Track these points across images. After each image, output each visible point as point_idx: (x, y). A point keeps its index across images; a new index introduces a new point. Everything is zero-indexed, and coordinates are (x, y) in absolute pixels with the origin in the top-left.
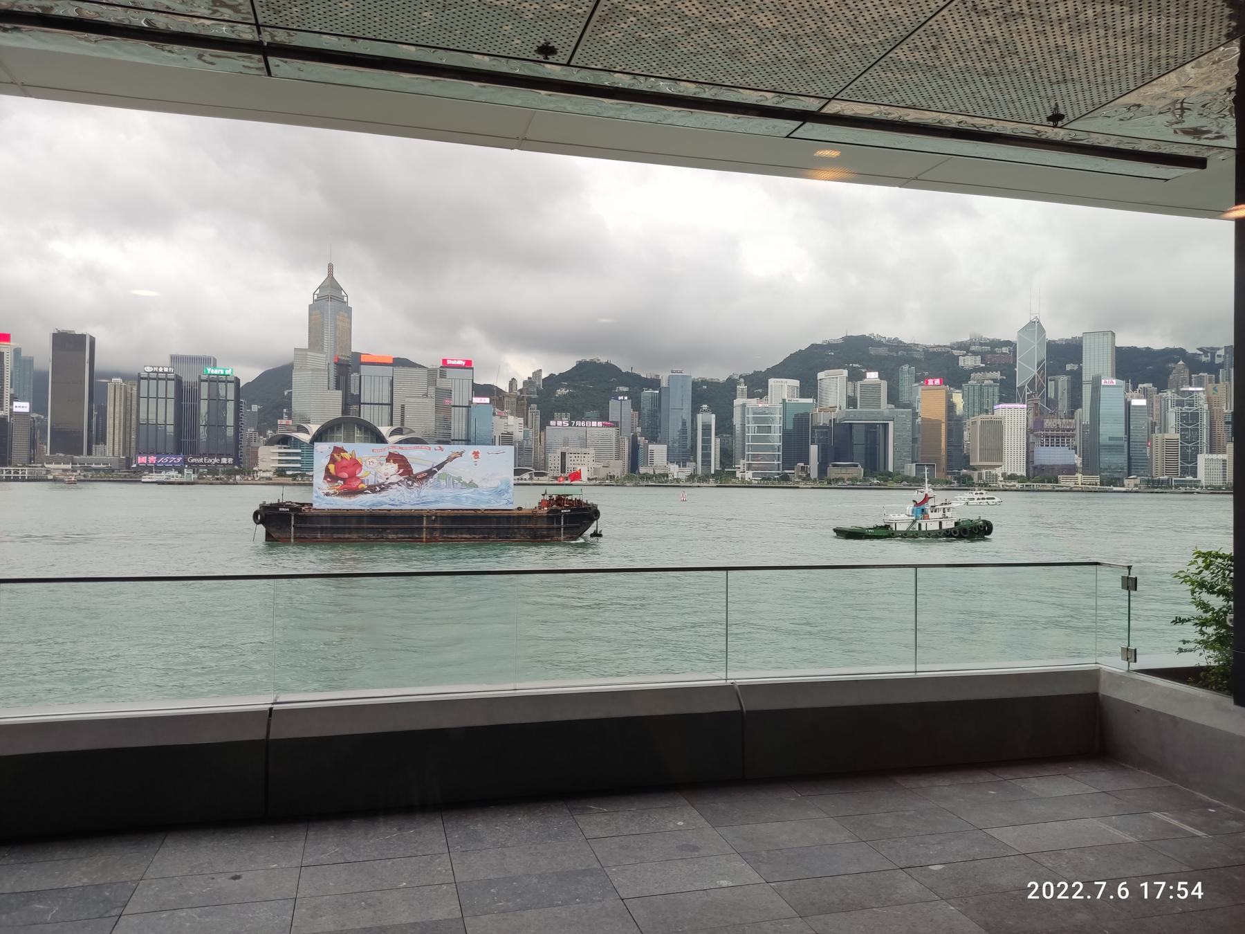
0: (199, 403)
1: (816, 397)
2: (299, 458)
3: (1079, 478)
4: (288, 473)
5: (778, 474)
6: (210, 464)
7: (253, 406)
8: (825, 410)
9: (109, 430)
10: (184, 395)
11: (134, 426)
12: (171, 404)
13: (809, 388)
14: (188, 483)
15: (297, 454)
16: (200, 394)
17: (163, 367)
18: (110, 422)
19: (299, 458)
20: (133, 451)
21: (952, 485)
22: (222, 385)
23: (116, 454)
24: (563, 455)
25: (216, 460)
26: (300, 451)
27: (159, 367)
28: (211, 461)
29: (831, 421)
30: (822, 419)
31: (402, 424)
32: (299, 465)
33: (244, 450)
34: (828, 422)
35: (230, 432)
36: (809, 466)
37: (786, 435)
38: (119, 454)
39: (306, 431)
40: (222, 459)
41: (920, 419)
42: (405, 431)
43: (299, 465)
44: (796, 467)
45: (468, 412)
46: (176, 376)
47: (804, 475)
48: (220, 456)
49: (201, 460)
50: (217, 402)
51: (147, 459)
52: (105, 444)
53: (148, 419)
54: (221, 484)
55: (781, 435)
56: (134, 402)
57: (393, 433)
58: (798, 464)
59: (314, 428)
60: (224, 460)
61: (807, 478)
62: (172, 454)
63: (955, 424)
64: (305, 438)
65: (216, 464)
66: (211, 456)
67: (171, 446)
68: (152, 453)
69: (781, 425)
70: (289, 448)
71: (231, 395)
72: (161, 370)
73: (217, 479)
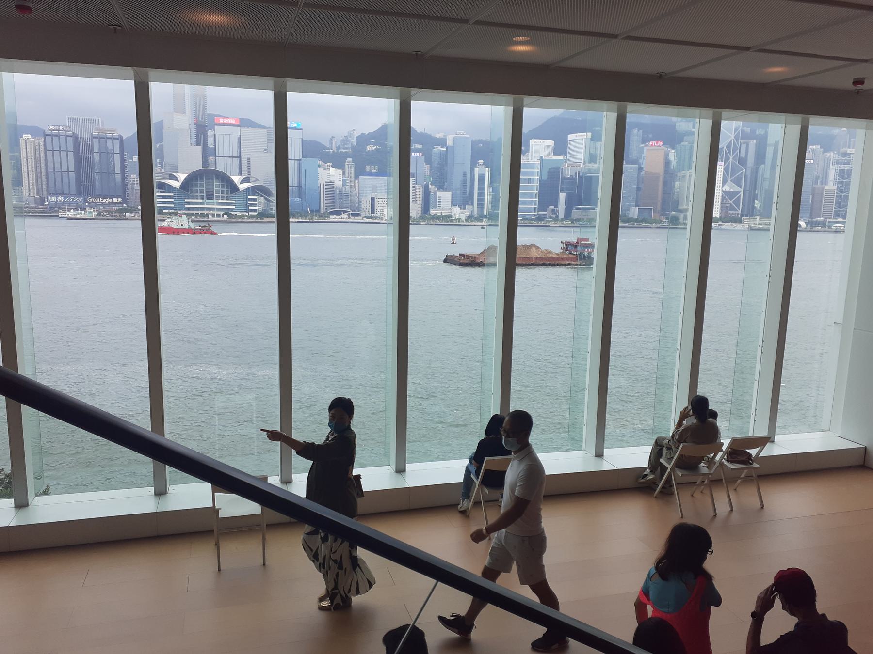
0: (93, 155)
1: (565, 154)
2: (172, 200)
3: (758, 220)
4: (164, 211)
5: (535, 215)
6: (105, 203)
7: (133, 157)
8: (572, 165)
9: (25, 175)
10: (80, 148)
11: (43, 172)
12: (71, 156)
13: (561, 148)
14: (90, 219)
15: (170, 197)
16: (93, 148)
17: (62, 127)
18: (24, 170)
19: (172, 200)
20: (45, 192)
21: (664, 224)
22: (109, 142)
23: (32, 194)
24: (373, 199)
25: (109, 200)
26: (172, 194)
27: (59, 126)
28: (105, 200)
29: (576, 173)
30: (569, 172)
31: (249, 174)
32: (173, 206)
33: (129, 192)
34: (574, 174)
35: (118, 177)
36: (557, 209)
37: (542, 183)
38: (34, 194)
39: (176, 179)
40: (114, 199)
41: (643, 172)
42: (252, 180)
43: (173, 206)
44: (548, 209)
45: (299, 165)
46: (73, 133)
47: (554, 216)
48: (112, 197)
49: (98, 200)
50: (106, 153)
51: (57, 198)
52: (23, 186)
53: (54, 168)
54: (115, 219)
55: (538, 185)
56: (42, 154)
57: (243, 181)
58: (550, 207)
59: (182, 177)
60: (115, 200)
61: (556, 219)
62: (75, 195)
63: (669, 175)
64: (176, 184)
65: (109, 203)
66: (105, 197)
67: (73, 190)
68: (61, 195)
69: (539, 177)
70: (164, 192)
71: (117, 149)
72: (61, 128)
73: (112, 216)
